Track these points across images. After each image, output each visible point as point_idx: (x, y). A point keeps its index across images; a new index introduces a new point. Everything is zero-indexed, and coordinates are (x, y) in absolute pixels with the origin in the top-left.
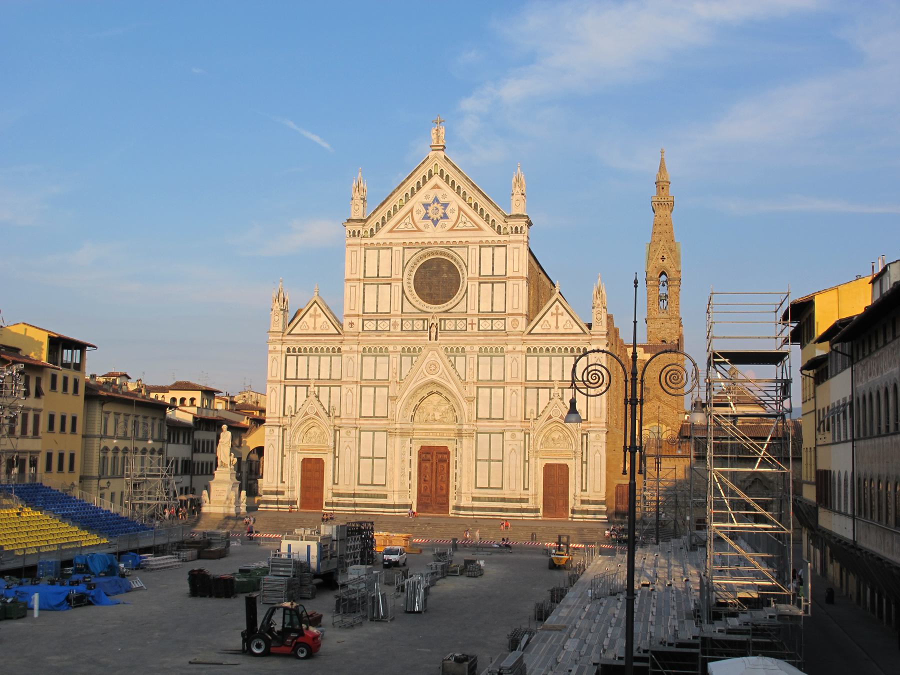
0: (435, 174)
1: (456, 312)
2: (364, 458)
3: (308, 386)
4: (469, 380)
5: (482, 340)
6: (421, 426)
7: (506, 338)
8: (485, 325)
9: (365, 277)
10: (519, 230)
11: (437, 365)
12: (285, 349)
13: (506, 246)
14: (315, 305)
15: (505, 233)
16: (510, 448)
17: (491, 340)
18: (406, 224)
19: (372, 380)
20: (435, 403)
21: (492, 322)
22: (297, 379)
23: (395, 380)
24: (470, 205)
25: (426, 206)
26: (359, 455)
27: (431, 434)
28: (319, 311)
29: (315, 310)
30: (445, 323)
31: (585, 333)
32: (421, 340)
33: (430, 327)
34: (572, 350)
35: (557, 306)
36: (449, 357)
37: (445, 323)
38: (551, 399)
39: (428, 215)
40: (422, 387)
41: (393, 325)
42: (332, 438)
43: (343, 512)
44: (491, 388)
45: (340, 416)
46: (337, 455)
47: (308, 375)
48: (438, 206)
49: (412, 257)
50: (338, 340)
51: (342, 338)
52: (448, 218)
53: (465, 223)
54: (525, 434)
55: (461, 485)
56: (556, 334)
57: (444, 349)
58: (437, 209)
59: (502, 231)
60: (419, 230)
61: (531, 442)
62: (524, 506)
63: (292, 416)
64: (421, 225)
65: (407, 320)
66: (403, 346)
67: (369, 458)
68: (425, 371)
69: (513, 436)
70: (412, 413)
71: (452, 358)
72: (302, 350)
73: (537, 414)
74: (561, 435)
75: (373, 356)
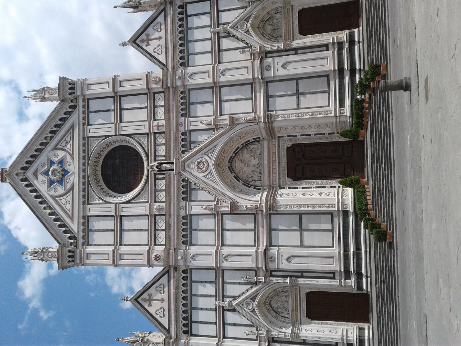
0: (24, 176)
1: (148, 145)
2: (301, 241)
3: (224, 310)
4: (213, 124)
5: (173, 114)
6: (266, 178)
7: (171, 89)
8: (160, 113)
9: (114, 245)
10: (70, 86)
11: (199, 160)
12: (184, 336)
13: (89, 99)
14: (140, 300)
15: (76, 101)
16: (281, 70)
17: (173, 104)
18: (66, 202)
19: (215, 234)
20: (242, 165)
21: (157, 107)
22: (216, 323)
23: (213, 207)
24: (51, 138)
25: (51, 183)
26: (297, 246)
27: (274, 167)
28: (145, 296)
29: (145, 300)
30: (159, 156)
31: (164, 10)
32: (174, 180)
33: (160, 170)
34: (180, 20)
35: (141, 41)
36: (190, 149)
37: (159, 156)
38: (229, 35)
39: (59, 180)
40: (223, 178)
41: (159, 212)
42: (280, 280)
43: (368, 265)
44: (221, 101)
45: (255, 271)
46: (299, 274)
47: (211, 310)
48: (51, 170)
49: (96, 195)
50: (174, 274)
51: (172, 269)
52: (63, 160)
53: (67, 143)
54: (267, 57)
55: (327, 126)
56: (166, 38)
57: (182, 154)
58: (54, 171)
59: (73, 104)
60: (72, 188)
61: (275, 48)
62: (346, 46)
63: (257, 330)
64: (69, 186)
65: (155, 196)
66: (181, 199)
67: (301, 235)
68: (204, 174)
69: (268, 68)
70: (252, 189)
71: (192, 145)
72: (184, 315)
73: (245, 48)
74: (268, 22)
75: (191, 233)
